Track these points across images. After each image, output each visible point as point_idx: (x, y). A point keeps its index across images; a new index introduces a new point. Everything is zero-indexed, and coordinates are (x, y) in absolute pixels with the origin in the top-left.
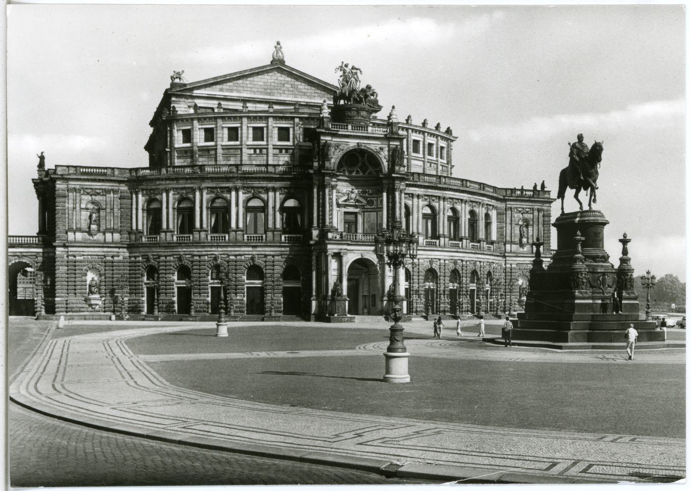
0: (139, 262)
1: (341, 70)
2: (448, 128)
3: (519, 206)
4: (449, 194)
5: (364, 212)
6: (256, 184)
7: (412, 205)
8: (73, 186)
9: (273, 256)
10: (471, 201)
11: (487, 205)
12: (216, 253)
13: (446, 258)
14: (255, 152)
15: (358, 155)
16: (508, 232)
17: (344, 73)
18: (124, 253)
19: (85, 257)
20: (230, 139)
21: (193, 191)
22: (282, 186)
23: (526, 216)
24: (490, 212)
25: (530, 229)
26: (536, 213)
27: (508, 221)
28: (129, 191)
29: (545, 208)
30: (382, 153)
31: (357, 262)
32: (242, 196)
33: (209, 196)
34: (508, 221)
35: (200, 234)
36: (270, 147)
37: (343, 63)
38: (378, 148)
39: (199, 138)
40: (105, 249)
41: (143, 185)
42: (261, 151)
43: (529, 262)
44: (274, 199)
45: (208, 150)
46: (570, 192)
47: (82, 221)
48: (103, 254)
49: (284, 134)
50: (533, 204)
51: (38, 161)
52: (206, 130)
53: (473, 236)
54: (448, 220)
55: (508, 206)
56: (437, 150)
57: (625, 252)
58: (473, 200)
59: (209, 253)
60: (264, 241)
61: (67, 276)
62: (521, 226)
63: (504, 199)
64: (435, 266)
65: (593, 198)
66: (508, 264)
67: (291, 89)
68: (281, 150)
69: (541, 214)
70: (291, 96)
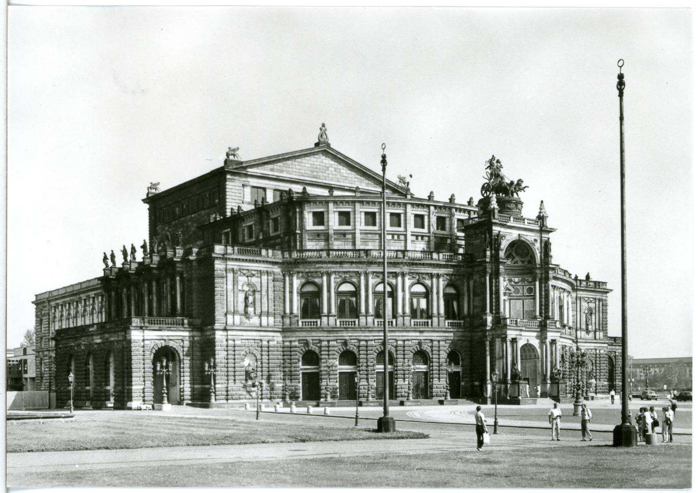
0: (296, 347)
5: (510, 299)
6: (423, 270)
8: (232, 267)
9: (439, 341)
14: (393, 237)
18: (278, 337)
19: (243, 341)
21: (358, 274)
22: (446, 272)
25: (593, 317)
27: (578, 310)
28: (281, 274)
29: (604, 298)
32: (408, 282)
35: (366, 319)
41: (299, 268)
42: (398, 237)
45: (344, 235)
48: (260, 338)
49: (419, 220)
52: (341, 213)
55: (579, 295)
59: (376, 338)
60: (357, 326)
68: (417, 236)
69: (601, 303)
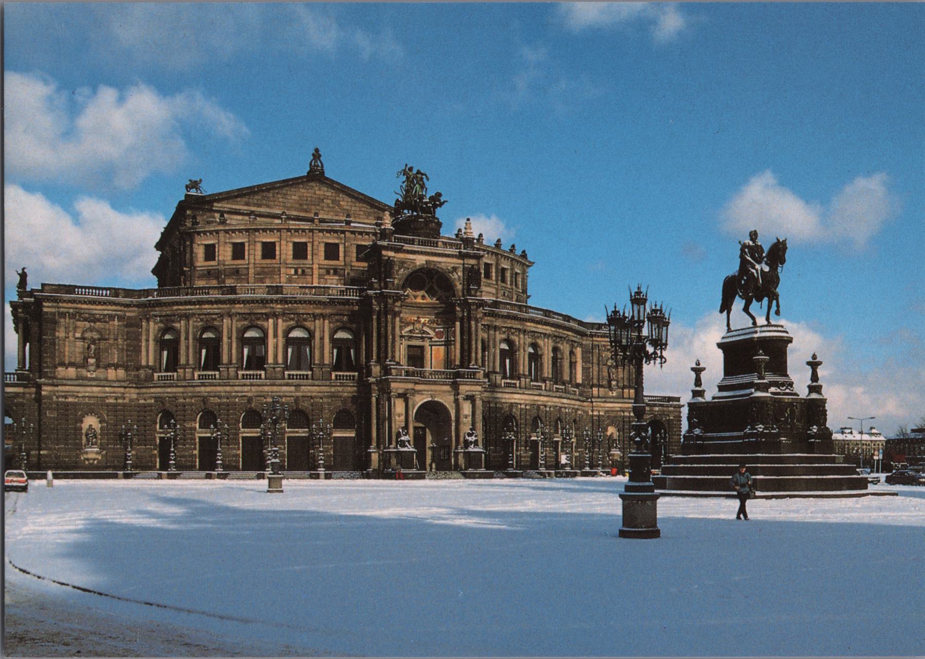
1: (404, 175)
2: (524, 252)
4: (530, 326)
5: (431, 346)
7: (488, 338)
10: (555, 336)
11: (572, 341)
12: (249, 394)
13: (527, 402)
14: (296, 272)
15: (424, 276)
17: (407, 178)
20: (264, 257)
27: (595, 360)
30: (455, 273)
31: (424, 406)
33: (240, 324)
35: (228, 371)
36: (315, 266)
37: (406, 165)
38: (449, 268)
39: (225, 254)
42: (303, 271)
44: (323, 329)
46: (738, 304)
49: (331, 251)
51: (18, 278)
53: (557, 377)
54: (529, 357)
56: (511, 277)
57: (815, 377)
58: (556, 334)
59: (240, 394)
62: (610, 367)
65: (774, 308)
67: (331, 205)
70: (332, 213)
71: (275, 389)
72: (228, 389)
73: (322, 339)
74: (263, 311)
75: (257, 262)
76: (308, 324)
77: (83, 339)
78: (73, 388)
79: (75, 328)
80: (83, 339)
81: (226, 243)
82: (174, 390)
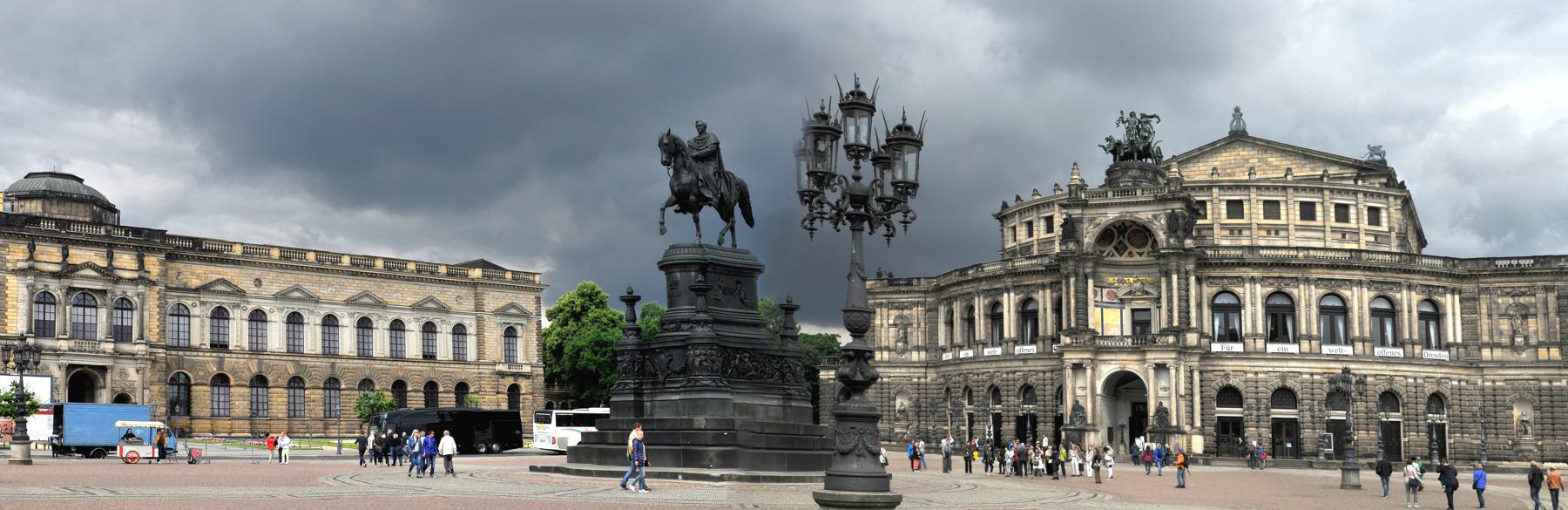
3: (1502, 285)
9: (1044, 372)
13: (1315, 371)
16: (1485, 327)
23: (1522, 300)
24: (1436, 298)
26: (1541, 295)
27: (1484, 309)
33: (987, 301)
34: (1484, 310)
40: (912, 370)
43: (1531, 377)
47: (890, 339)
50: (1534, 278)
59: (985, 370)
61: (874, 400)
63: (1471, 276)
64: (1290, 383)
66: (1488, 381)
69: (1552, 297)
71: (1008, 364)
72: (978, 366)
73: (1045, 310)
74: (999, 286)
75: (1041, 237)
76: (1034, 296)
77: (895, 325)
78: (888, 370)
79: (888, 316)
80: (895, 325)
81: (1022, 223)
82: (949, 369)
